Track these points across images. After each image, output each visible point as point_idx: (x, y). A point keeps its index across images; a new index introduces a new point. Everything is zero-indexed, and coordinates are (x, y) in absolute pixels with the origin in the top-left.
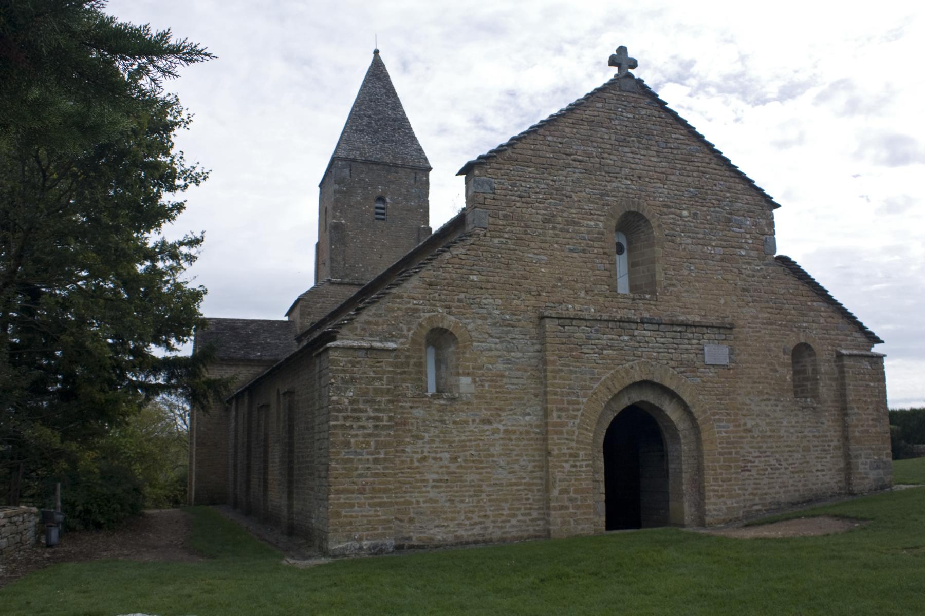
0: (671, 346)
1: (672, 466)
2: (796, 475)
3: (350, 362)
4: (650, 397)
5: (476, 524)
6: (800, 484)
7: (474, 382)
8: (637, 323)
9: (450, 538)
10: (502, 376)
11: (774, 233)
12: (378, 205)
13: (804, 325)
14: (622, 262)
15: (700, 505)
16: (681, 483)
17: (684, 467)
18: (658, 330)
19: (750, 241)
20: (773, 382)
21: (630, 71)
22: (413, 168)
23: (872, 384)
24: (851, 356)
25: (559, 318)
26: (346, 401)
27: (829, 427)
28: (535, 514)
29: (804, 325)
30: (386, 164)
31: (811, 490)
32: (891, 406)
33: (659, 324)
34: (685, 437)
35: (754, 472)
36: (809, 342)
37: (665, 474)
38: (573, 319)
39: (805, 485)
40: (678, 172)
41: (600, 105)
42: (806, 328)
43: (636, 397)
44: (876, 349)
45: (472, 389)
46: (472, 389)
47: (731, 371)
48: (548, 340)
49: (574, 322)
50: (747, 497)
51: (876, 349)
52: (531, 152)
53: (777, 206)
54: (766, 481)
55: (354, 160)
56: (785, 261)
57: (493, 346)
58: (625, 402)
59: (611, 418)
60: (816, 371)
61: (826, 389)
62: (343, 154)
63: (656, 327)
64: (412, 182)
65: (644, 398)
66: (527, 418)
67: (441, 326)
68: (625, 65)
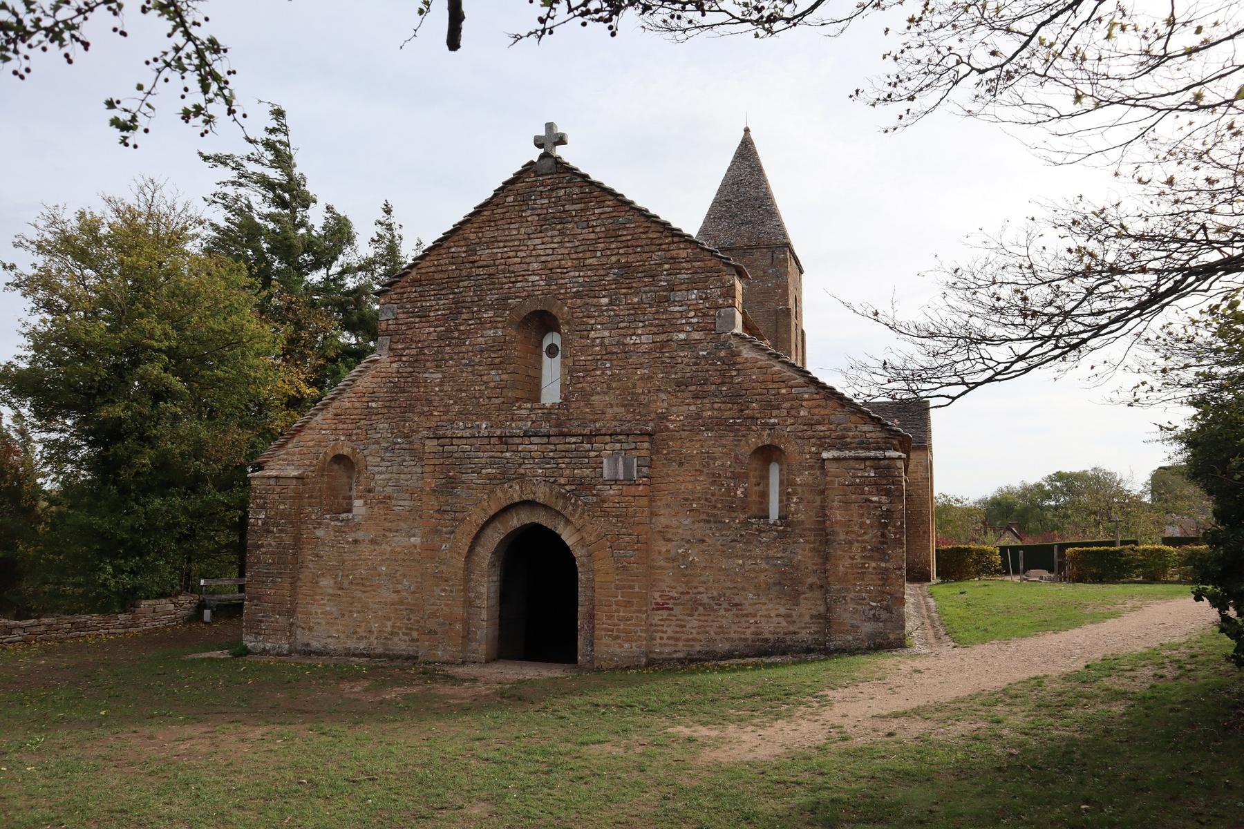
2: (743, 620)
4: (542, 519)
5: (361, 638)
6: (749, 631)
7: (365, 504)
10: (390, 498)
13: (772, 421)
19: (695, 320)
20: (713, 499)
22: (768, 247)
23: (875, 499)
24: (836, 459)
29: (772, 421)
30: (741, 248)
31: (767, 640)
33: (549, 436)
34: (583, 565)
35: (677, 611)
40: (599, 254)
42: (774, 424)
45: (363, 511)
46: (363, 511)
50: (665, 641)
52: (433, 269)
54: (696, 624)
59: (497, 540)
63: (545, 440)
64: (769, 261)
65: (535, 520)
66: (412, 539)
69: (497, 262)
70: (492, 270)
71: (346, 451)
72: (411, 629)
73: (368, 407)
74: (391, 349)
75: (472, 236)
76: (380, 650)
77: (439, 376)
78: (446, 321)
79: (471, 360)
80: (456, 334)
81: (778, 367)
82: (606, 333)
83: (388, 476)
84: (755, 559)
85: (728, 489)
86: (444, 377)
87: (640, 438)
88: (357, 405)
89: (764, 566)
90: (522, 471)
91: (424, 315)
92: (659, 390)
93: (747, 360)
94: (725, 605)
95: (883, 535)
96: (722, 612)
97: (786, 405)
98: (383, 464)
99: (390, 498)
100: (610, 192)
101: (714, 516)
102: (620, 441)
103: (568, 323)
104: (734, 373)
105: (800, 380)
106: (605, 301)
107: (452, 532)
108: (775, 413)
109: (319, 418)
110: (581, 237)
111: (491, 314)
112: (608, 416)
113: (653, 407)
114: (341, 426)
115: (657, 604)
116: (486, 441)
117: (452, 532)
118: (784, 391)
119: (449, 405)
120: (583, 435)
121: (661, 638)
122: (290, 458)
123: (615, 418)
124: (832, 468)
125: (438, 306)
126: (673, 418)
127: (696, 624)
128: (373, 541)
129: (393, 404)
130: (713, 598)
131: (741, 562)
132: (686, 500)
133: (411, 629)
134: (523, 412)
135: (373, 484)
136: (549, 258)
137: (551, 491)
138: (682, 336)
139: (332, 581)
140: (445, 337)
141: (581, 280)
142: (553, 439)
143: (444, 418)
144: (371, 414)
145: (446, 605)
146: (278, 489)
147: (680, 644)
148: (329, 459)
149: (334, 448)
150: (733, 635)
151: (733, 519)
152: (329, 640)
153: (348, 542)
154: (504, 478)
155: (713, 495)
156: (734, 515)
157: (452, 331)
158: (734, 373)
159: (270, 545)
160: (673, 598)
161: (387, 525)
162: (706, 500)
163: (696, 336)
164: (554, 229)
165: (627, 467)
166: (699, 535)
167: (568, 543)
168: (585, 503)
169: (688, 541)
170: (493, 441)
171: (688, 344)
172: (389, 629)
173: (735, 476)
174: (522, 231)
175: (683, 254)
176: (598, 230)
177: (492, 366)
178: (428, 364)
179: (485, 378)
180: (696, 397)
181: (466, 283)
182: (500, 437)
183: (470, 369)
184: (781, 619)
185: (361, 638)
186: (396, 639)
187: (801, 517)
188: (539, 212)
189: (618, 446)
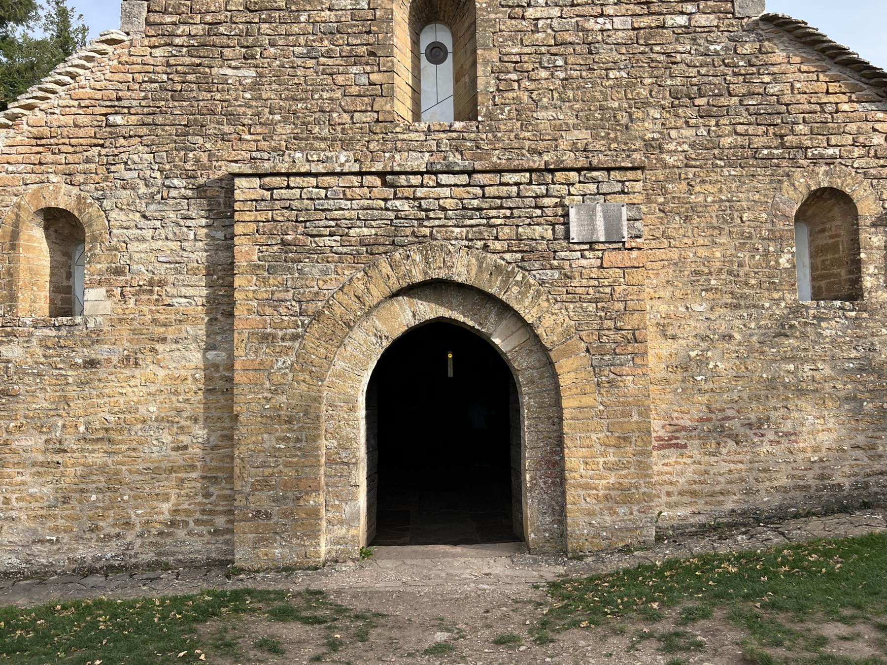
0: (493, 213)
5: (109, 537)
6: (810, 474)
7: (110, 294)
8: (422, 174)
9: (62, 561)
13: (830, 151)
18: (469, 185)
25: (261, 176)
29: (830, 151)
34: (531, 382)
36: (838, 183)
38: (288, 175)
39: (822, 477)
43: (430, 310)
45: (107, 306)
46: (107, 306)
47: (635, 253)
48: (237, 216)
49: (294, 181)
50: (675, 498)
57: (148, 233)
63: (464, 179)
65: (443, 312)
67: (53, 205)
71: (62, 202)
72: (212, 512)
74: (148, 23)
76: (149, 556)
77: (252, 73)
82: (556, 12)
83: (159, 244)
84: (814, 362)
85: (766, 254)
86: (261, 75)
87: (630, 175)
88: (82, 120)
90: (427, 231)
92: (646, 104)
94: (771, 436)
97: (852, 127)
98: (143, 223)
99: (161, 283)
101: (743, 297)
102: (594, 181)
104: (767, 79)
107: (294, 337)
112: (563, 145)
113: (637, 128)
115: (660, 439)
116: (355, 180)
117: (294, 337)
118: (845, 107)
119: (273, 123)
120: (531, 171)
121: (669, 494)
123: (574, 148)
126: (672, 146)
129: (160, 120)
131: (791, 367)
132: (697, 273)
133: (212, 512)
134: (413, 136)
135: (122, 260)
137: (480, 262)
138: (682, 20)
142: (479, 178)
143: (264, 144)
144: (115, 136)
145: (287, 465)
151: (777, 302)
153: (74, 366)
154: (391, 242)
155: (740, 265)
156: (776, 296)
158: (767, 79)
160: (684, 428)
162: (730, 273)
166: (723, 329)
168: (542, 283)
170: (369, 180)
172: (166, 516)
173: (775, 237)
178: (227, 52)
179: (340, 79)
182: (381, 174)
183: (310, 63)
184: (859, 453)
186: (181, 533)
189: (592, 188)
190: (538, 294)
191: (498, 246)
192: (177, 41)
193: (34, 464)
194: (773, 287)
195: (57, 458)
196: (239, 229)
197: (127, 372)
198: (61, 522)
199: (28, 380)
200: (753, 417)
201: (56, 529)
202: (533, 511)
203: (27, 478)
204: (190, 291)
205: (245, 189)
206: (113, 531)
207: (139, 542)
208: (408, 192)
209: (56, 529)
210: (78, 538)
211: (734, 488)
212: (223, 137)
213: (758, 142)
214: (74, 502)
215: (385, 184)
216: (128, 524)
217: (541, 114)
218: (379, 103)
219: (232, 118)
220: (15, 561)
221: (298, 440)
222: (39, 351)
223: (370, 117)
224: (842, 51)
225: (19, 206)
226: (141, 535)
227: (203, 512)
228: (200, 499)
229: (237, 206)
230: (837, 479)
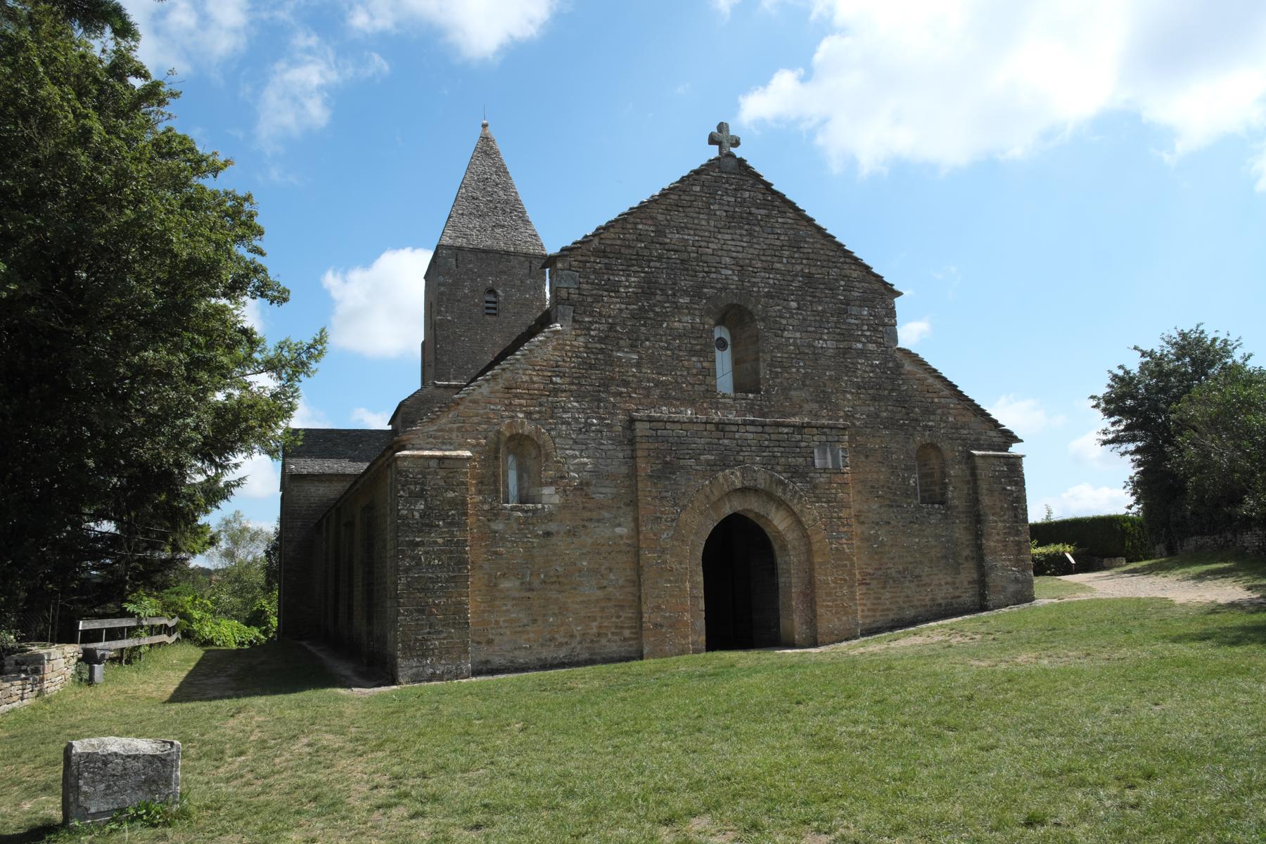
1: (781, 580)
3: (421, 473)
4: (752, 505)
5: (561, 645)
10: (588, 484)
11: (894, 325)
12: (488, 298)
14: (723, 361)
15: (812, 622)
16: (790, 599)
17: (794, 580)
21: (732, 150)
24: (983, 456)
26: (417, 515)
27: (960, 532)
28: (627, 633)
32: (1036, 515)
37: (775, 588)
39: (933, 600)
41: (698, 188)
44: (1015, 449)
45: (557, 499)
46: (557, 499)
49: (668, 426)
51: (1015, 449)
52: (618, 242)
53: (899, 294)
55: (460, 248)
56: (906, 352)
58: (727, 510)
60: (944, 474)
61: (956, 496)
62: (447, 241)
63: (760, 429)
65: (747, 506)
66: (618, 530)
68: (726, 144)
69: (690, 249)
70: (685, 256)
71: (528, 428)
72: (622, 627)
73: (552, 382)
74: (574, 321)
75: (660, 217)
78: (638, 300)
79: (669, 344)
80: (651, 315)
81: (931, 380)
82: (798, 335)
85: (904, 478)
86: (641, 358)
89: (934, 543)
91: (613, 288)
93: (909, 372)
95: (1016, 516)
96: (907, 584)
97: (939, 411)
99: (588, 484)
100: (791, 205)
102: (825, 434)
103: (763, 320)
105: (946, 392)
106: (794, 305)
107: (673, 520)
108: (932, 417)
109: (485, 390)
110: (768, 242)
111: (687, 300)
114: (517, 401)
116: (702, 427)
117: (673, 520)
120: (794, 426)
122: (446, 435)
124: (979, 462)
125: (630, 282)
127: (888, 595)
128: (572, 533)
130: (899, 572)
132: (873, 487)
133: (622, 627)
136: (740, 256)
137: (771, 476)
138: (860, 346)
139: (517, 583)
140: (639, 316)
141: (771, 282)
142: (767, 429)
146: (442, 473)
147: (878, 614)
148: (503, 439)
149: (510, 426)
150: (916, 603)
152: (517, 653)
153: (537, 536)
157: (646, 311)
159: (436, 543)
161: (586, 514)
163: (871, 347)
164: (741, 228)
165: (835, 458)
167: (781, 528)
169: (877, 524)
170: (709, 427)
171: (862, 353)
172: (595, 630)
173: (907, 468)
174: (712, 223)
175: (855, 274)
176: (782, 237)
177: (692, 352)
178: (622, 342)
180: (874, 399)
181: (658, 264)
182: (717, 424)
185: (561, 645)
186: (604, 641)
187: (956, 502)
188: (726, 208)
189: (824, 438)
190: (801, 497)
191: (779, 468)
192: (592, 333)
193: (514, 599)
194: (908, 496)
195: (528, 594)
196: (639, 453)
197: (569, 540)
198: (532, 635)
199: (509, 544)
200: (901, 568)
201: (529, 640)
202: (795, 623)
203: (509, 607)
204: (604, 490)
205: (641, 429)
206: (564, 640)
207: (579, 647)
208: (731, 435)
209: (529, 640)
210: (542, 645)
211: (893, 607)
212: (620, 394)
213: (898, 416)
214: (539, 622)
215: (717, 429)
216: (572, 636)
217: (793, 393)
218: (708, 379)
219: (626, 384)
220: (503, 661)
221: (676, 581)
222: (515, 526)
223: (703, 388)
224: (935, 371)
225: (499, 432)
226: (580, 643)
227: (617, 627)
228: (614, 619)
229: (638, 439)
230: (940, 601)
